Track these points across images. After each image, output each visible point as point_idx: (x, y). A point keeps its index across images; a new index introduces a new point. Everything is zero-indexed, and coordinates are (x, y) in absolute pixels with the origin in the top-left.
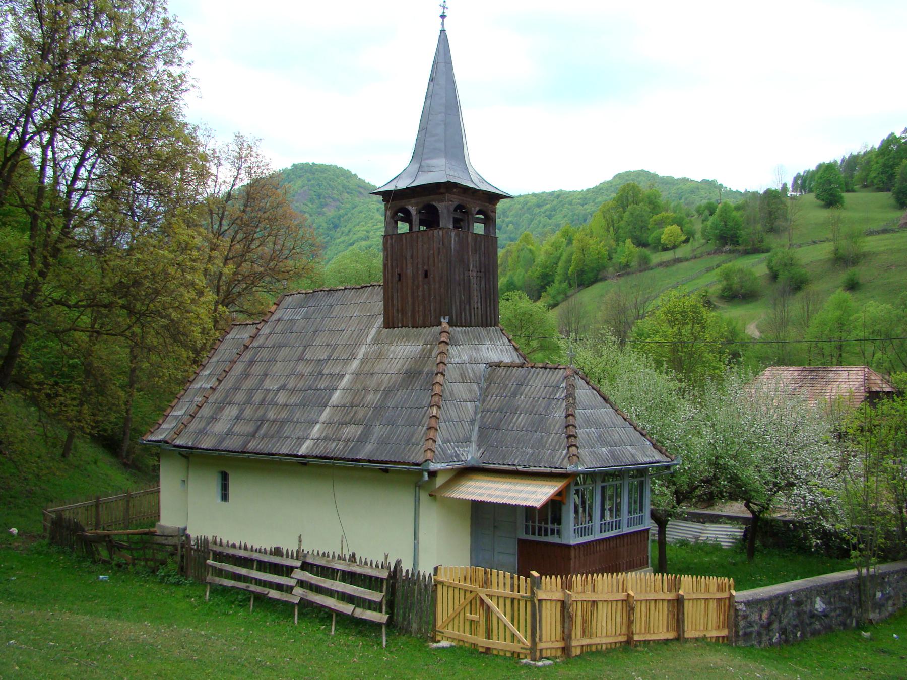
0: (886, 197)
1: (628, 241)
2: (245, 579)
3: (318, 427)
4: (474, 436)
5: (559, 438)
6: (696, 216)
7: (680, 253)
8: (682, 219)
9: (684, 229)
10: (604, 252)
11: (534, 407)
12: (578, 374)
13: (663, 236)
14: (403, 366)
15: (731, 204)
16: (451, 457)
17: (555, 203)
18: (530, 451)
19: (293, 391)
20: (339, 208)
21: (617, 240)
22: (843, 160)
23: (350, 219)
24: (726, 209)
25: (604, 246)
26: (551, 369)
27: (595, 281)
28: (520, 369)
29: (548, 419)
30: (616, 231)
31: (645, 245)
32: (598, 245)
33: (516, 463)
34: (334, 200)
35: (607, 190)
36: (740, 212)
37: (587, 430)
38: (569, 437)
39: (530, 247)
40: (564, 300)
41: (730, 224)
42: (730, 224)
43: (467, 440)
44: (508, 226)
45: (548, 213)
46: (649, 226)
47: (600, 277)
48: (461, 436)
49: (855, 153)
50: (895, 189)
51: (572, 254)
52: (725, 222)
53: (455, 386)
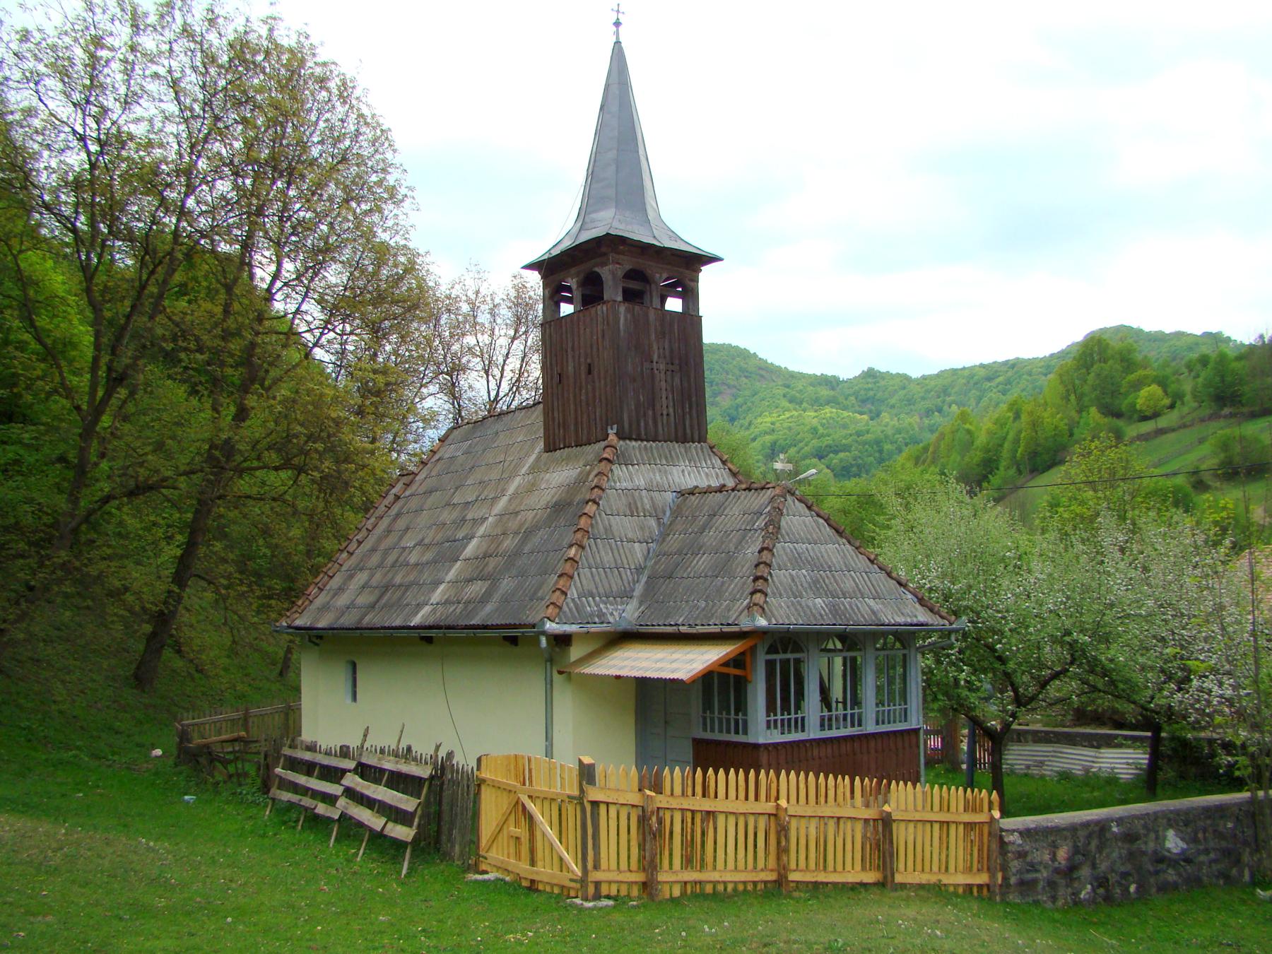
1: (1093, 410)
2: (305, 791)
3: (442, 587)
4: (639, 589)
5: (744, 583)
6: (1186, 374)
7: (1162, 422)
8: (1166, 378)
9: (1169, 390)
10: (1063, 426)
11: (722, 543)
12: (793, 494)
13: (1138, 401)
14: (553, 497)
15: (1229, 352)
16: (592, 615)
18: (703, 604)
19: (428, 546)
20: (735, 397)
21: (1080, 411)
23: (749, 409)
24: (1222, 358)
25: (1062, 419)
26: (756, 490)
28: (718, 494)
29: (737, 557)
30: (1080, 398)
31: (1118, 415)
32: (1053, 419)
33: (679, 622)
34: (729, 386)
36: (1243, 363)
37: (794, 573)
38: (756, 579)
39: (967, 426)
41: (1229, 379)
42: (1229, 379)
43: (626, 595)
44: (950, 407)
46: (1122, 390)
48: (615, 589)
51: (1020, 432)
53: (615, 521)
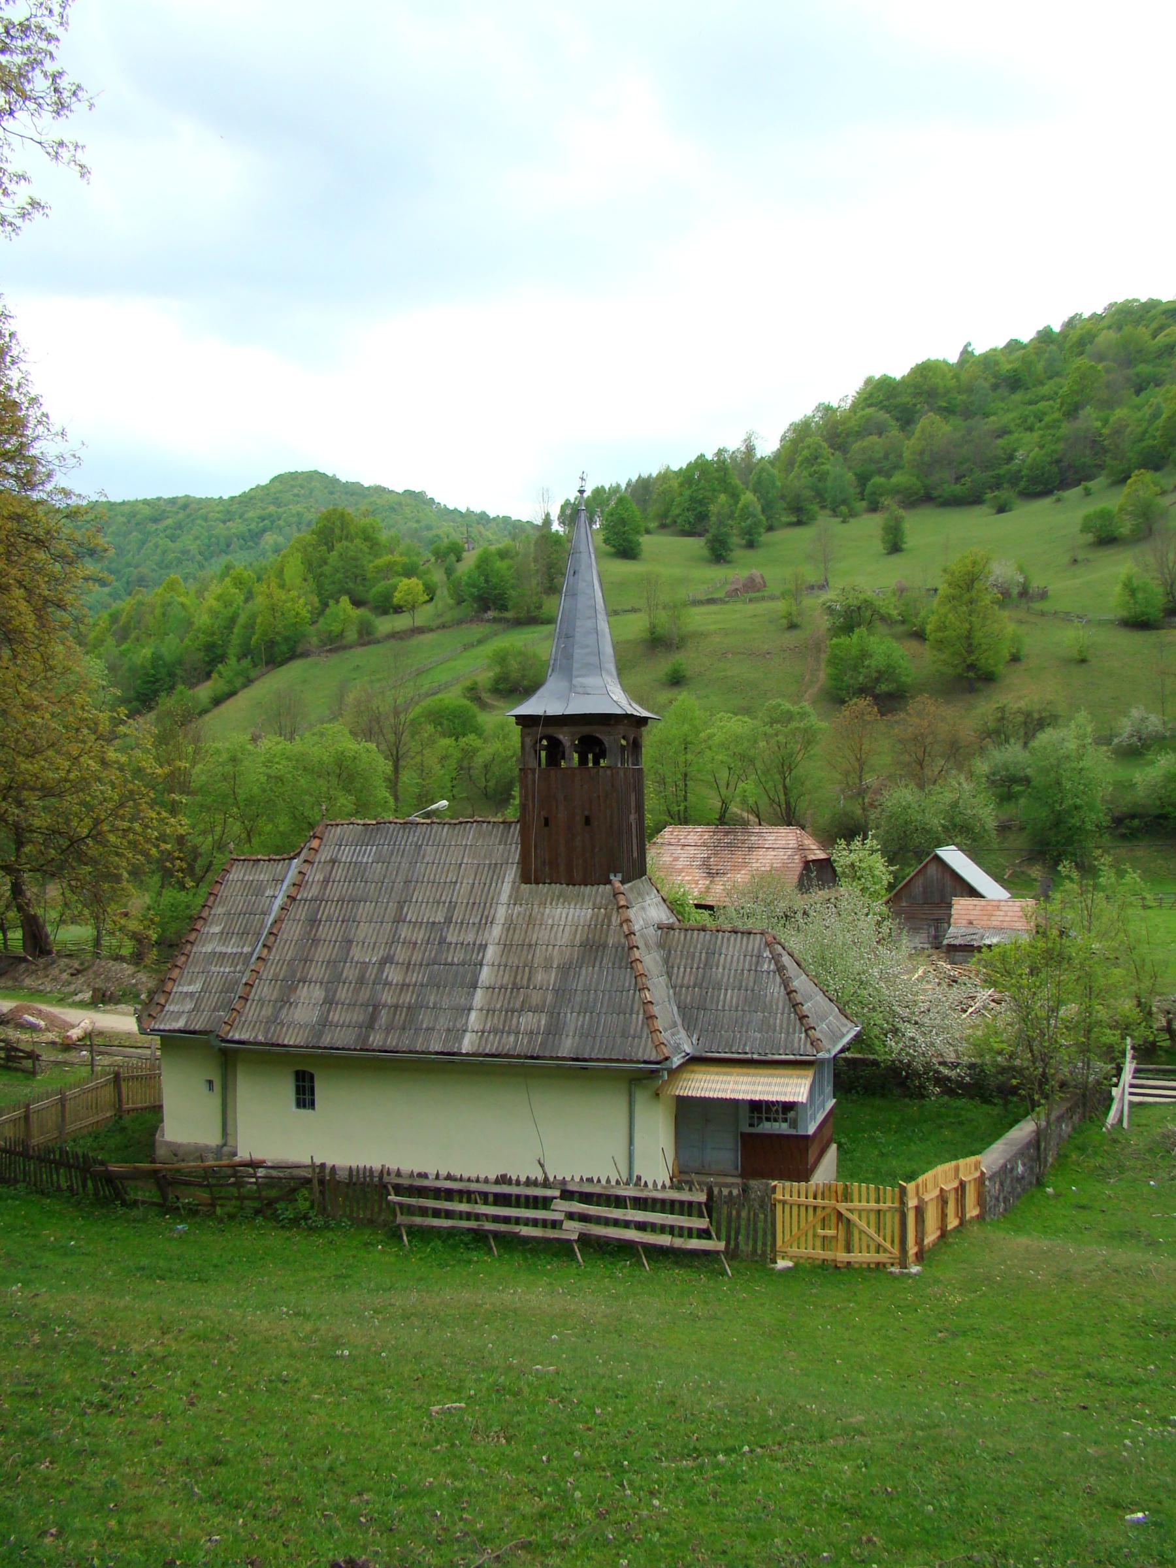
0: (696, 545)
17: (181, 516)
22: (628, 485)
27: (293, 656)
35: (262, 501)
40: (245, 686)
45: (169, 532)
47: (299, 650)
49: (645, 475)
50: (709, 536)
52: (487, 576)
